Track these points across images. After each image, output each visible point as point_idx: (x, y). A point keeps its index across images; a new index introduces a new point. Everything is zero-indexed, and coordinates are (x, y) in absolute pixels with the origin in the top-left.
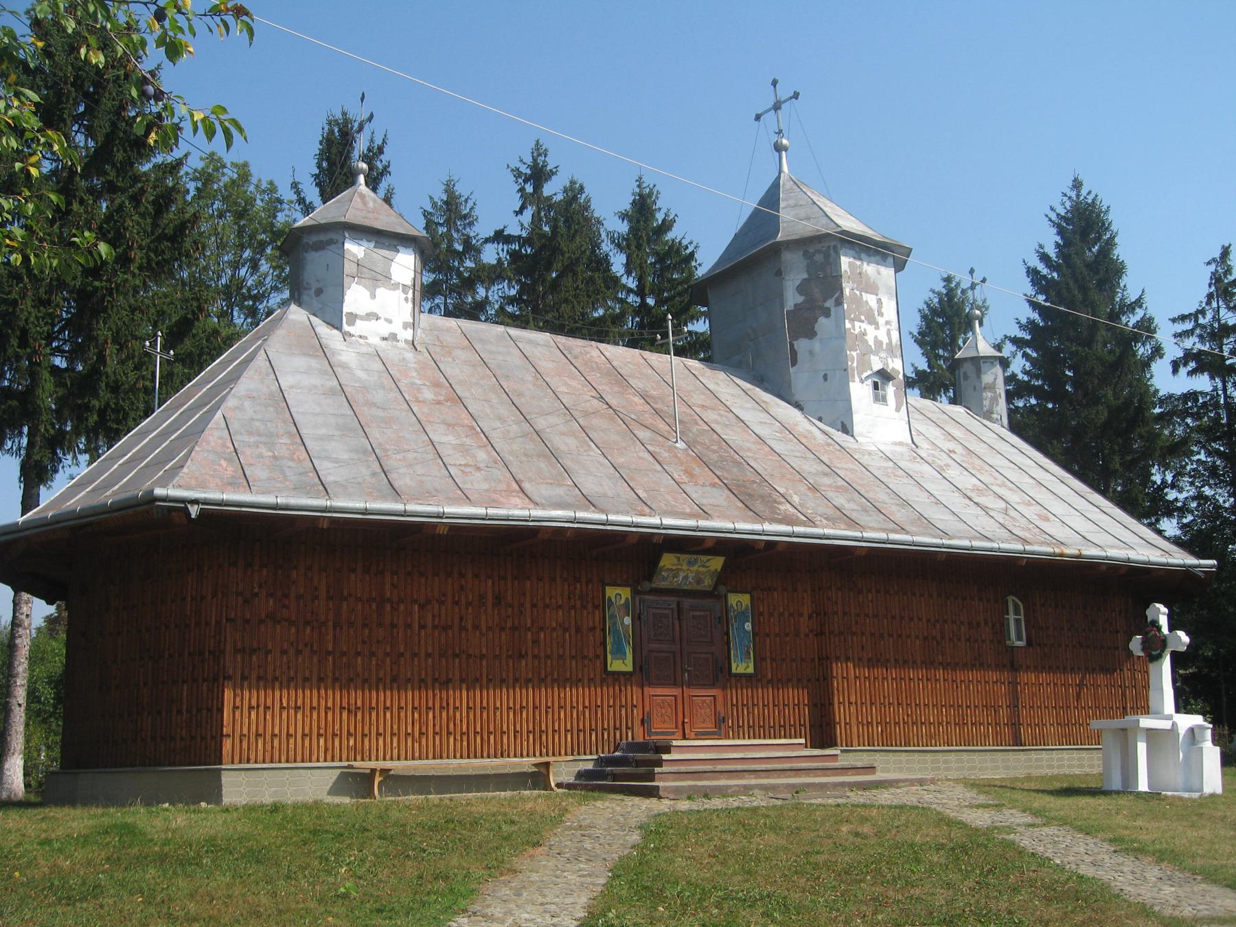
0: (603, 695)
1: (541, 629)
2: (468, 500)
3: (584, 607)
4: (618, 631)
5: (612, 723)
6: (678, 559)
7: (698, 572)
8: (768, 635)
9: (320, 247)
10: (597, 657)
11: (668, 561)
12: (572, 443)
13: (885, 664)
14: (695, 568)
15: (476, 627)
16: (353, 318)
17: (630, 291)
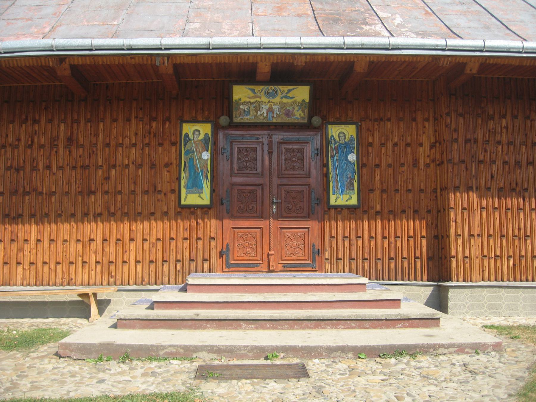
0: (178, 227)
1: (114, 166)
3: (161, 144)
4: (195, 166)
5: (187, 254)
6: (253, 90)
7: (283, 105)
8: (377, 166)
10: (173, 191)
11: (241, 93)
13: (522, 193)
14: (277, 99)
15: (48, 167)
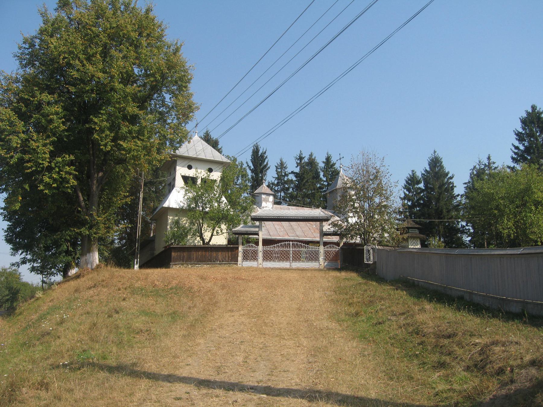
2: (280, 236)
9: (258, 196)
12: (296, 227)
16: (263, 207)
17: (325, 181)
